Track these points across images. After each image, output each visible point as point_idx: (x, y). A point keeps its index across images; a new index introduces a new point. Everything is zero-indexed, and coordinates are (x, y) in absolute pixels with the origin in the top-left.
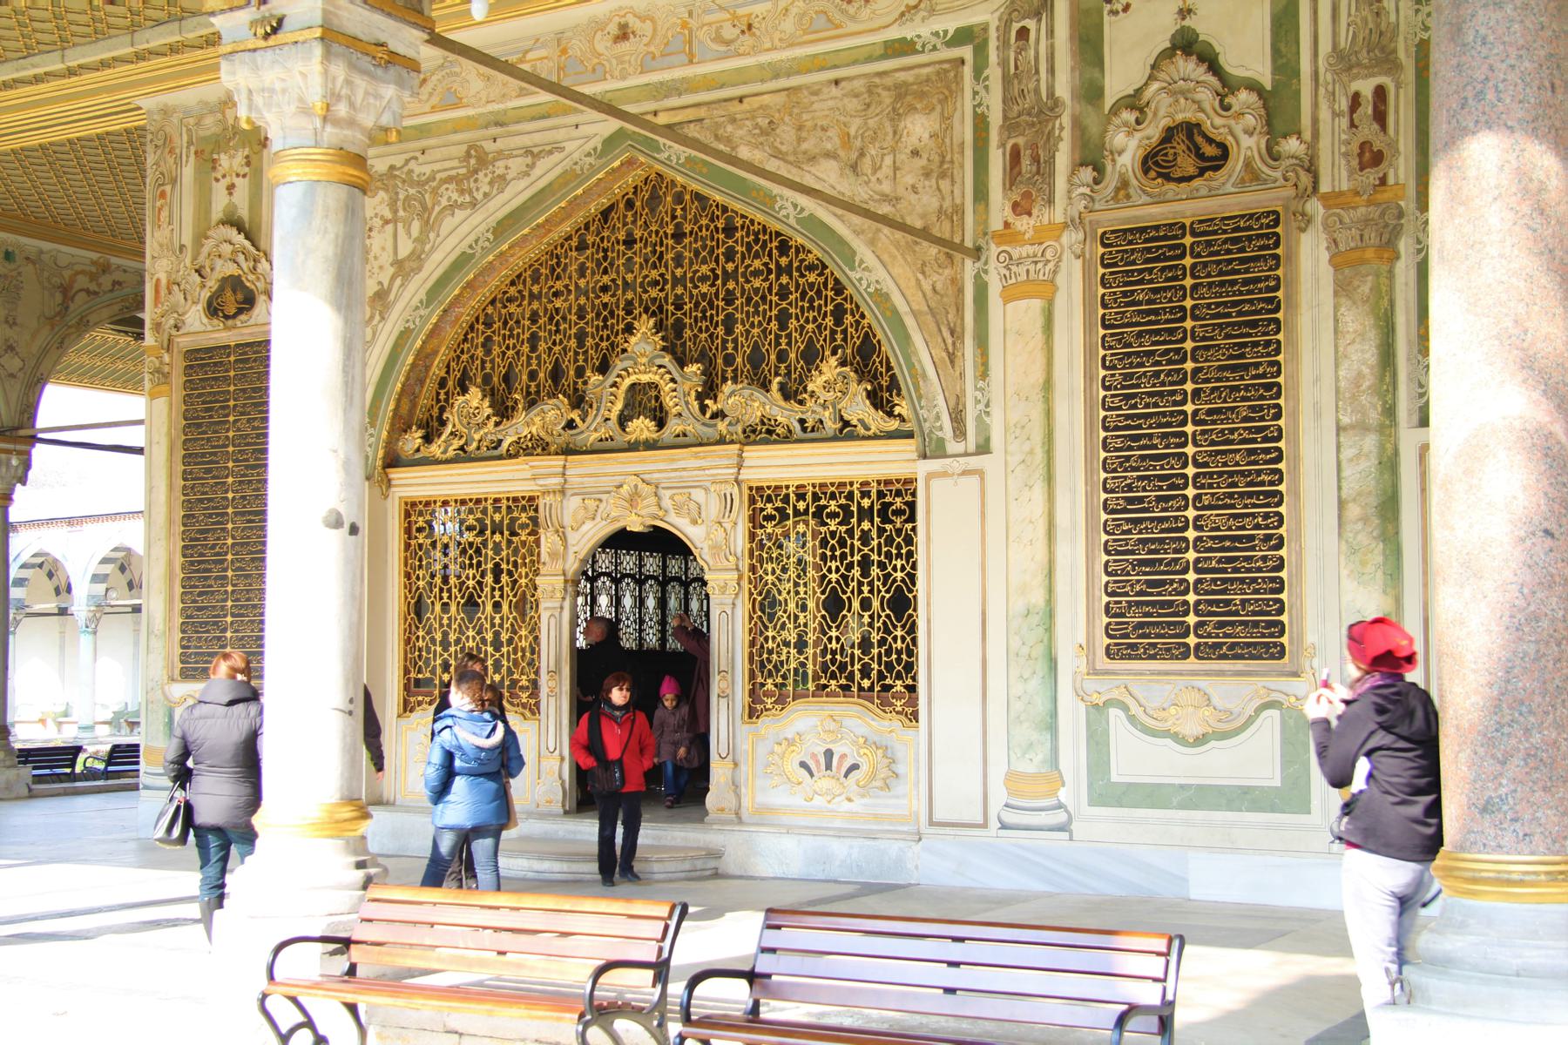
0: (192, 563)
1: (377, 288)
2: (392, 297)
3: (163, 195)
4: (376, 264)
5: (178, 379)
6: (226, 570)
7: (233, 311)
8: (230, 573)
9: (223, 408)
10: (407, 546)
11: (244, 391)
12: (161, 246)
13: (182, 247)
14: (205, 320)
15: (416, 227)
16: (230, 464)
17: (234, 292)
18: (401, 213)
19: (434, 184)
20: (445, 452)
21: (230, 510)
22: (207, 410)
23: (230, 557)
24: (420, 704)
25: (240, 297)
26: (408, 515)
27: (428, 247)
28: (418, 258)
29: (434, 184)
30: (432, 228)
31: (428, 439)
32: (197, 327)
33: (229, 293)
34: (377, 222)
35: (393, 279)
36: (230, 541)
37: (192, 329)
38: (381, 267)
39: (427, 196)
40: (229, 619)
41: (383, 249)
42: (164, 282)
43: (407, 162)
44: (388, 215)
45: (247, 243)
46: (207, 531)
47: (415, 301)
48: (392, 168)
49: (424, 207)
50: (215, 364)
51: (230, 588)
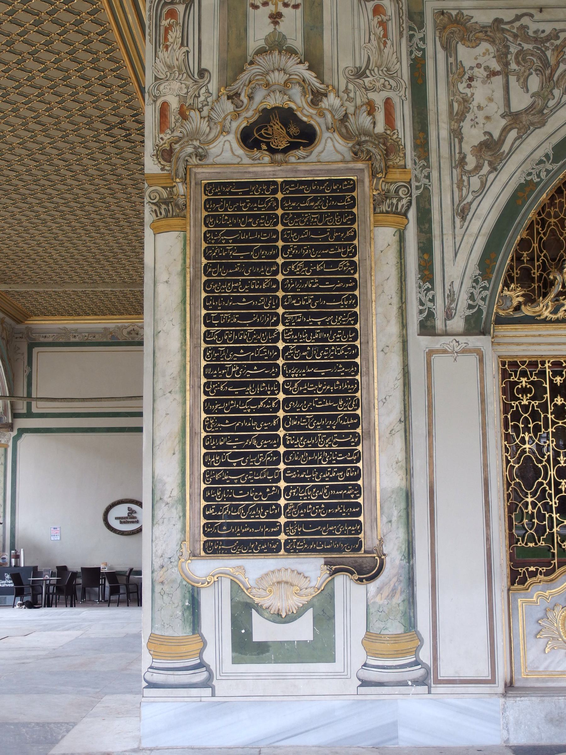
0: (221, 420)
1: (483, 138)
2: (506, 148)
3: (172, 14)
4: (481, 115)
5: (196, 214)
6: (277, 428)
7: (283, 145)
8: (281, 433)
9: (268, 248)
10: (506, 408)
11: (300, 232)
12: (170, 67)
13: (202, 72)
14: (240, 151)
15: (534, 83)
16: (281, 311)
17: (285, 124)
18: (513, 66)
19: (558, 42)
20: (555, 312)
21: (281, 362)
22: (240, 250)
23: (281, 414)
24: (533, 574)
25: (294, 130)
26: (505, 374)
27: (551, 103)
28: (538, 114)
29: (558, 42)
30: (557, 85)
31: (530, 300)
32: (227, 157)
33: (277, 126)
34: (481, 73)
35: (505, 131)
36: (281, 396)
37: (218, 160)
38: (488, 118)
39: (549, 53)
40: (282, 484)
41: (491, 100)
42: (174, 104)
43: (518, 18)
44: (495, 66)
45: (310, 76)
46: (246, 384)
47: (539, 154)
48: (498, 21)
49: (546, 64)
50: (253, 201)
51: (282, 449)
